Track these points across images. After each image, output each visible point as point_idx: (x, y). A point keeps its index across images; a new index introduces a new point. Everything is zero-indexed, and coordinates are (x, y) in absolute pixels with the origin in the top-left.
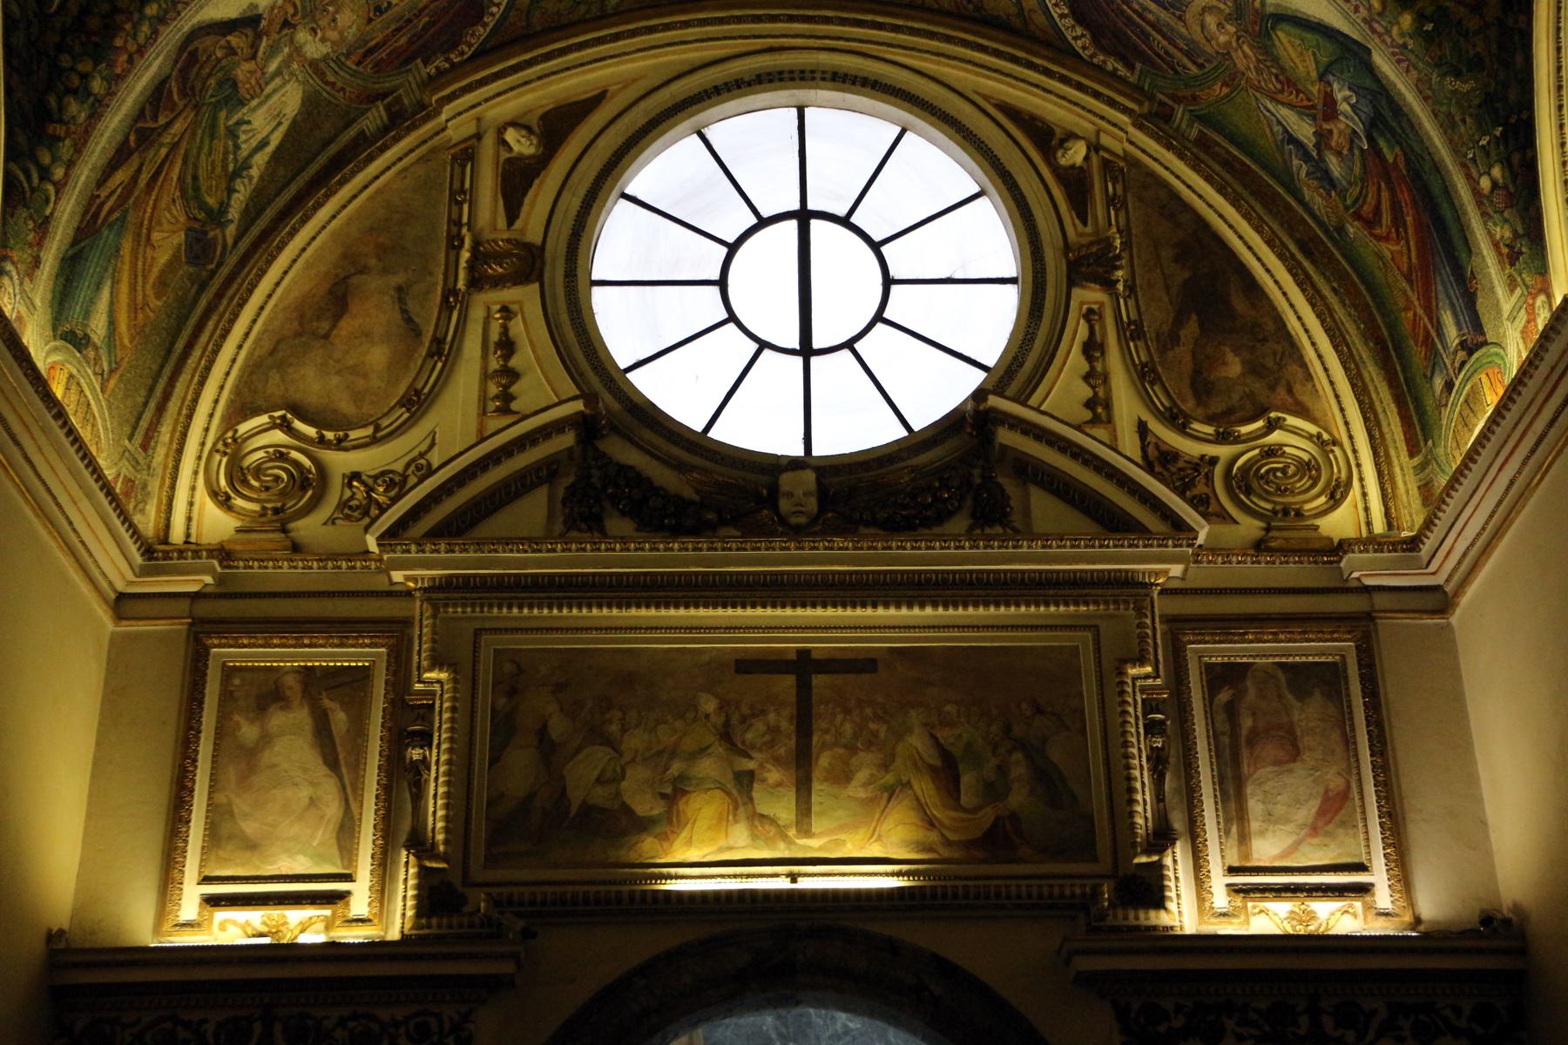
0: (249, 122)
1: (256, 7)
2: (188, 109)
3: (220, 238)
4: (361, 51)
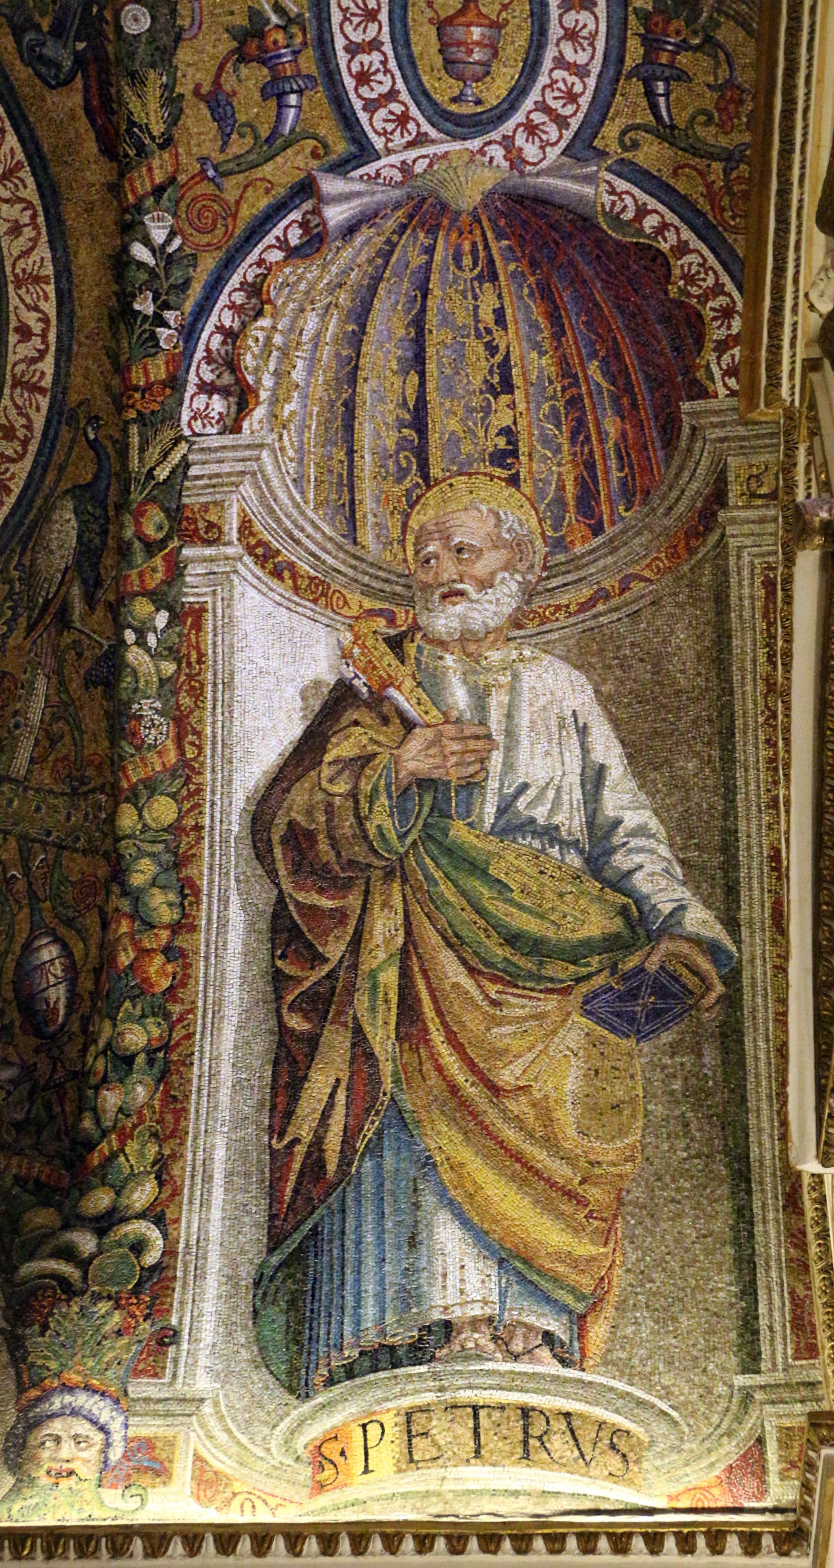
0: (525, 787)
1: (317, 684)
2: (377, 886)
3: (685, 948)
4: (571, 516)
